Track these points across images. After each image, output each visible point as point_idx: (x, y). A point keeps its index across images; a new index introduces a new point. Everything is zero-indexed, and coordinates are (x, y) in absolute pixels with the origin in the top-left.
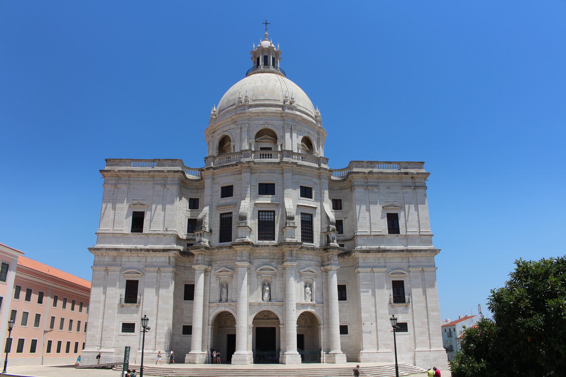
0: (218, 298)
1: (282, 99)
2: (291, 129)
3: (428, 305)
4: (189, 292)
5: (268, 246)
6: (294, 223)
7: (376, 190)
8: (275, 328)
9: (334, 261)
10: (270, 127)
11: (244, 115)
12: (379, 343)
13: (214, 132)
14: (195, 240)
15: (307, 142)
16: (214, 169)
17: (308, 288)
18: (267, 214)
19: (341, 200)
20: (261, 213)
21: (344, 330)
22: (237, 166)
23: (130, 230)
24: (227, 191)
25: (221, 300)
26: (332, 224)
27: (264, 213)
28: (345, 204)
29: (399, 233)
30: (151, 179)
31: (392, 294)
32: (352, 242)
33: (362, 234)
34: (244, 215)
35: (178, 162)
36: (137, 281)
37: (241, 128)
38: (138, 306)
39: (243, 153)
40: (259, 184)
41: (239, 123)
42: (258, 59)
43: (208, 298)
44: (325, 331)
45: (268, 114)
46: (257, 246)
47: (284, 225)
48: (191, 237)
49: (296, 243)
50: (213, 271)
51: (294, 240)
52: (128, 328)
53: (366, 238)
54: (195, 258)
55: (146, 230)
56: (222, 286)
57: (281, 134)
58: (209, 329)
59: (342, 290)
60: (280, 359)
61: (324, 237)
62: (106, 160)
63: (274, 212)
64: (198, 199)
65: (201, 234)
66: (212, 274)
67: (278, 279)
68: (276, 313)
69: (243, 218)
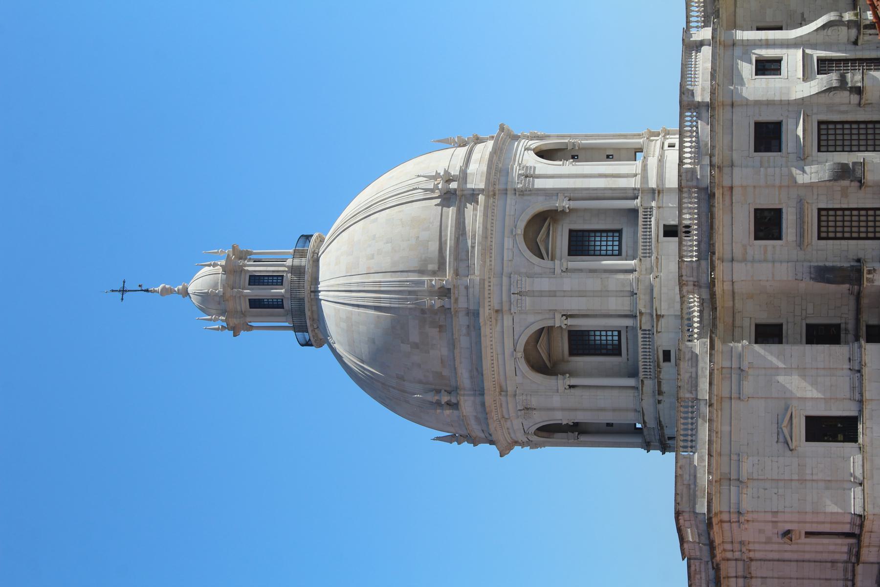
2: (527, 177)
10: (522, 225)
11: (487, 284)
13: (502, 391)
22: (714, 194)
24: (768, 224)
30: (726, 405)
35: (682, 347)
40: (756, 150)
41: (505, 298)
42: (255, 304)
45: (489, 227)
47: (855, 98)
57: (541, 198)
61: (867, 38)
63: (820, 123)
65: (869, 272)
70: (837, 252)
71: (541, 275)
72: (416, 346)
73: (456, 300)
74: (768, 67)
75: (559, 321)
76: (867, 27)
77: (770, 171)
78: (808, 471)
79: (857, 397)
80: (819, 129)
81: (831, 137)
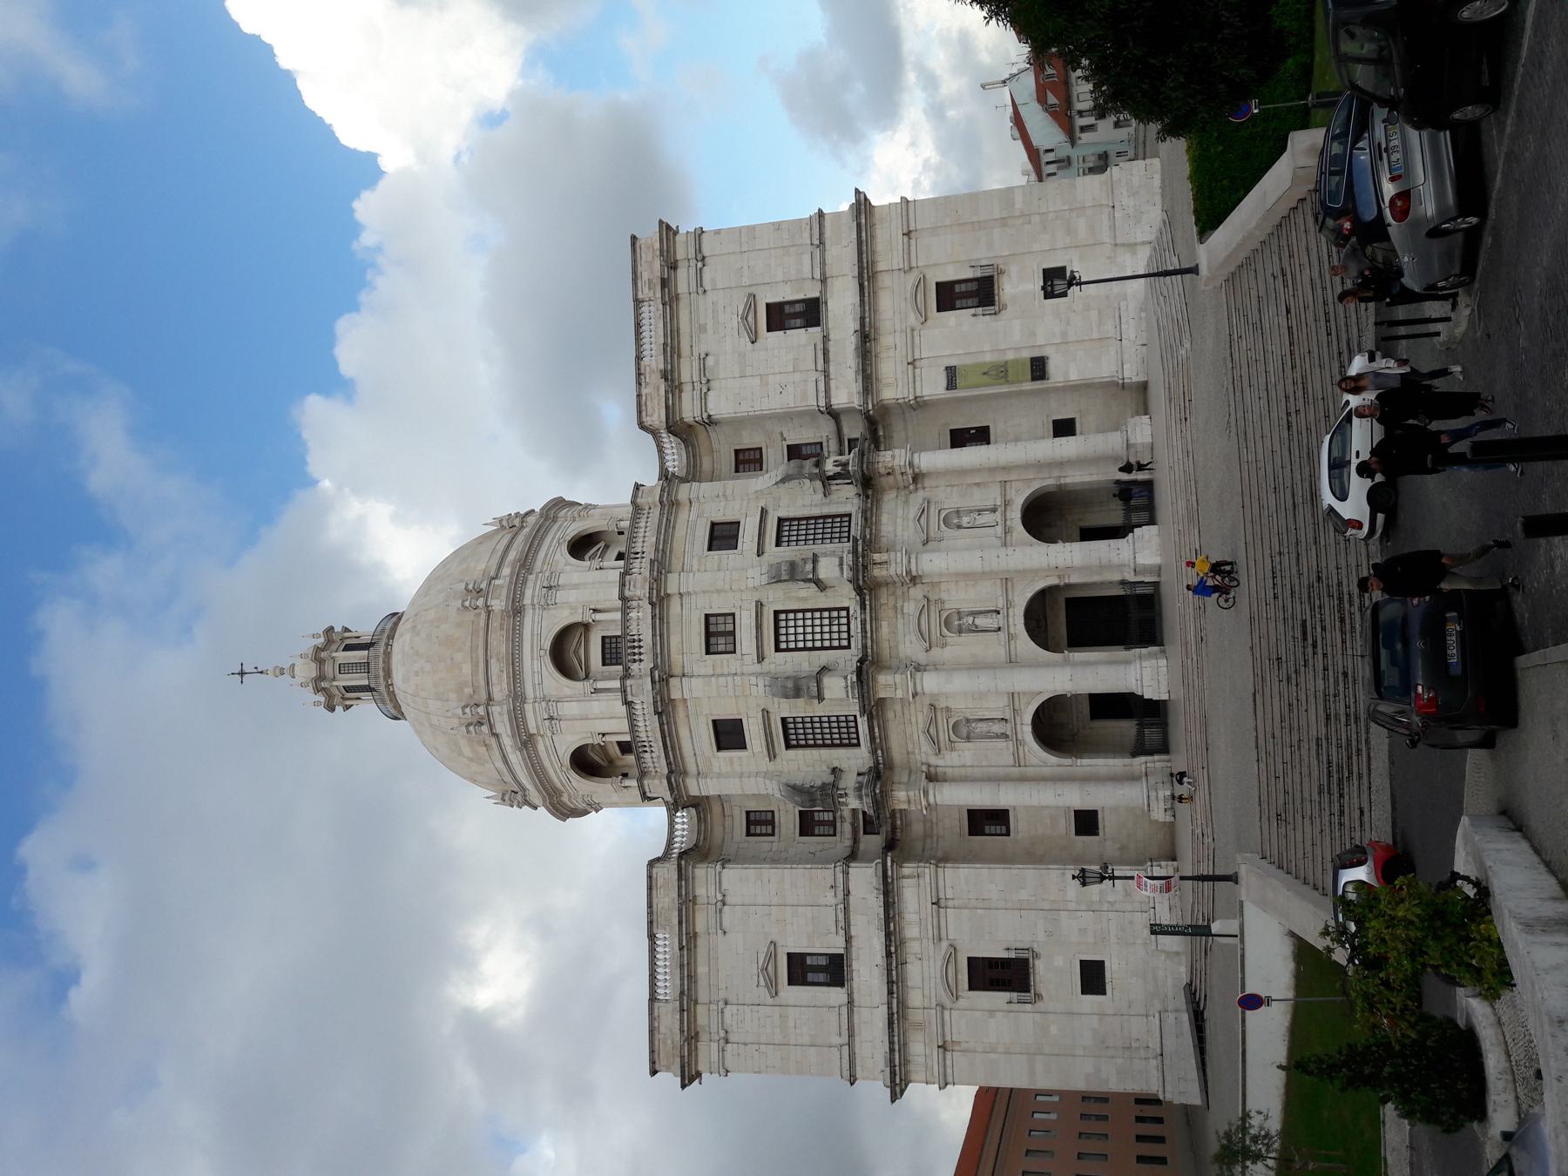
0: (1000, 744)
1: (470, 615)
2: (550, 588)
3: (997, 215)
4: (986, 821)
5: (863, 623)
6: (805, 561)
7: (710, 361)
8: (1068, 600)
9: (893, 457)
10: (547, 645)
12: (1095, 335)
14: (854, 811)
15: (581, 546)
16: (671, 772)
17: (965, 520)
18: (783, 631)
19: (737, 452)
20: (783, 646)
21: (1064, 428)
23: (838, 989)
25: (1005, 736)
26: (802, 467)
27: (783, 638)
28: (748, 440)
29: (817, 299)
31: (972, 311)
32: (843, 418)
33: (822, 394)
34: (790, 684)
36: (969, 959)
37: (551, 718)
38: (1036, 956)
39: (630, 698)
42: (348, 689)
43: (1001, 771)
44: (1070, 472)
46: (865, 647)
48: (847, 827)
49: (855, 552)
50: (934, 761)
51: (848, 559)
52: (1093, 977)
53: (833, 384)
54: (904, 806)
55: (836, 945)
56: (968, 738)
58: (1086, 764)
59: (960, 438)
60: (1147, 580)
62: (654, 1072)
63: (777, 613)
64: (748, 813)
65: (841, 796)
66: (940, 762)
67: (944, 596)
68: (1029, 595)
69: (795, 688)
70: (808, 765)
71: (570, 699)
72: (470, 759)
73: (491, 727)
74: (723, 536)
75: (598, 740)
76: (829, 478)
77: (722, 680)
78: (791, 1024)
79: (842, 932)
80: (777, 621)
81: (792, 630)
